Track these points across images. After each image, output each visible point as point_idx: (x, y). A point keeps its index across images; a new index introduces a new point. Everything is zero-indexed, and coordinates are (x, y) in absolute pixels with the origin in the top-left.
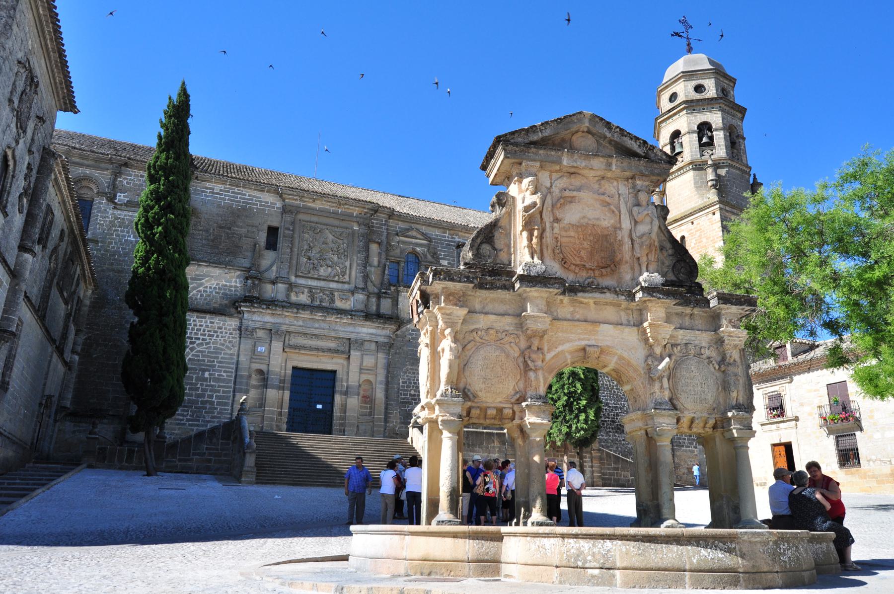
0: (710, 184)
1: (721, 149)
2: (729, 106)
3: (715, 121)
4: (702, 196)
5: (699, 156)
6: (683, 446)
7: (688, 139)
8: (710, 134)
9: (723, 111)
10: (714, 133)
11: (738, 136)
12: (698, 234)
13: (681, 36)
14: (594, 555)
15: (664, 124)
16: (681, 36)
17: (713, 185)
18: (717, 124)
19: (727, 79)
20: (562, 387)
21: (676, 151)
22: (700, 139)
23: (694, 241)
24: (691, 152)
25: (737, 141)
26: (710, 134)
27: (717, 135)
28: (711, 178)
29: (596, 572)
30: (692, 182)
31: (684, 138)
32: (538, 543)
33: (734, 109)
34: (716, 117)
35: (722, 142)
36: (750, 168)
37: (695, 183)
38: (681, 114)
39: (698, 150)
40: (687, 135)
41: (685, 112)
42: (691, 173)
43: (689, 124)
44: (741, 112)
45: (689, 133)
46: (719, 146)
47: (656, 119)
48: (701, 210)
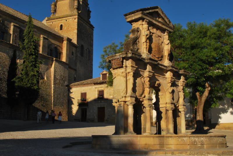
0: (75, 7)
4: (71, 11)
6: (56, 106)
12: (68, 25)
14: (199, 141)
20: (28, 81)
23: (66, 28)
28: (76, 5)
29: (200, 145)
30: (68, 4)
32: (181, 139)
36: (88, 5)
37: (69, 5)
48: (70, 16)
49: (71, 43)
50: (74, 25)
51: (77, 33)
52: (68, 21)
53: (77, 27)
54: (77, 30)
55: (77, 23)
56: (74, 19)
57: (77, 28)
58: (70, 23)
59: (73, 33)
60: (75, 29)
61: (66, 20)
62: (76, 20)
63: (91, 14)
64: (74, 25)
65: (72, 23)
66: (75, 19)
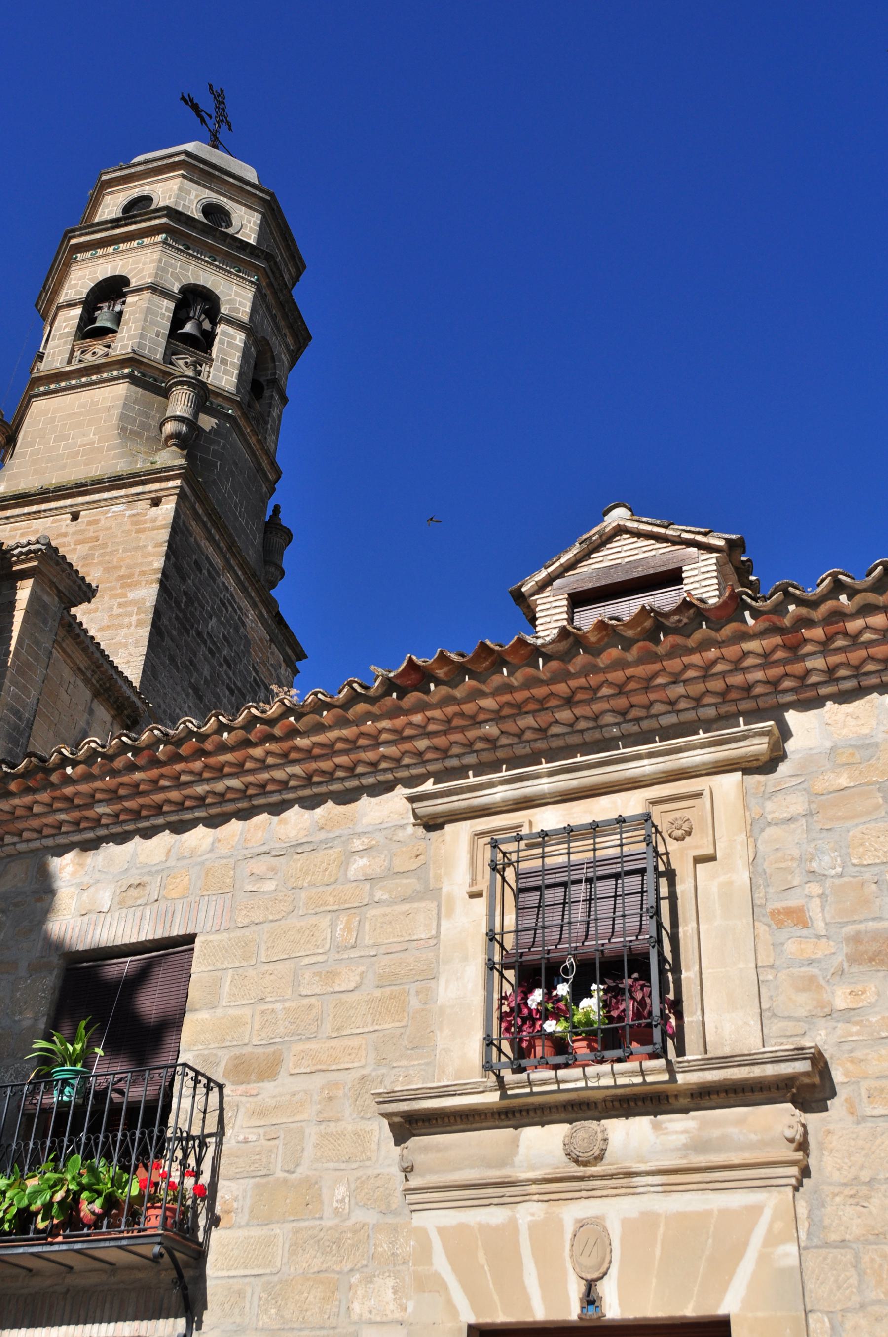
0: (169, 428)
1: (226, 372)
2: (275, 293)
3: (231, 302)
5: (159, 356)
7: (144, 305)
8: (207, 325)
9: (259, 290)
10: (221, 328)
11: (274, 383)
13: (203, 121)
15: (88, 254)
16: (203, 121)
17: (176, 435)
18: (237, 310)
19: (288, 247)
21: (97, 324)
22: (177, 322)
24: (142, 336)
25: (267, 393)
26: (207, 325)
27: (224, 333)
28: (178, 413)
30: (116, 412)
31: (130, 300)
33: (285, 316)
34: (237, 294)
35: (235, 358)
37: (123, 417)
38: (146, 241)
39: (163, 342)
40: (146, 294)
41: (161, 237)
42: (122, 389)
43: (161, 269)
44: (295, 335)
45: (154, 288)
46: (224, 362)
47: (68, 235)
49: (85, 650)
50: (137, 548)
51: (158, 613)
52: (90, 523)
53: (159, 563)
54: (161, 582)
55: (164, 535)
56: (144, 505)
57: (164, 572)
58: (101, 535)
59: (116, 611)
60: (143, 573)
61: (75, 517)
62: (168, 507)
63: (290, 558)
64: (137, 548)
65: (128, 532)
66: (156, 502)
